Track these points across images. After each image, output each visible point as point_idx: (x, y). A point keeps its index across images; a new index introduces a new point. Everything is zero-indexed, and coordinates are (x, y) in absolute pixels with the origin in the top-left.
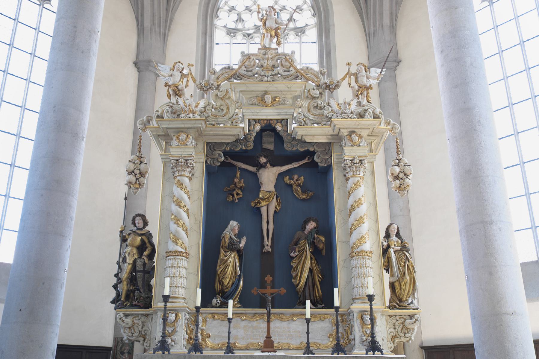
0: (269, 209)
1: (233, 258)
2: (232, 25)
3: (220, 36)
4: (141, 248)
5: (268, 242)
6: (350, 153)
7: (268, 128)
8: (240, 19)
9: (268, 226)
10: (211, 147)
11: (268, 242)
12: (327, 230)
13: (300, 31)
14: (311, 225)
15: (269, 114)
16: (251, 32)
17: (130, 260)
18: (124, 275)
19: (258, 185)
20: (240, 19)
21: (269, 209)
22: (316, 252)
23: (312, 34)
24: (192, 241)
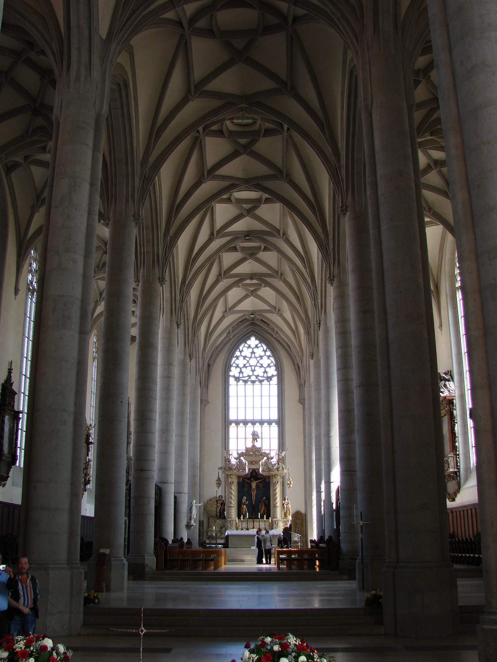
0: (254, 493)
1: (245, 506)
2: (237, 375)
3: (232, 381)
4: (222, 504)
5: (254, 502)
6: (275, 480)
7: (254, 470)
8: (241, 372)
9: (254, 498)
10: (239, 477)
11: (254, 502)
12: (268, 499)
13: (269, 379)
14: (264, 498)
15: (254, 467)
16: (246, 379)
17: (219, 508)
18: (218, 511)
19: (251, 487)
20: (241, 372)
21: (254, 493)
22: (265, 505)
23: (275, 380)
24: (234, 502)
